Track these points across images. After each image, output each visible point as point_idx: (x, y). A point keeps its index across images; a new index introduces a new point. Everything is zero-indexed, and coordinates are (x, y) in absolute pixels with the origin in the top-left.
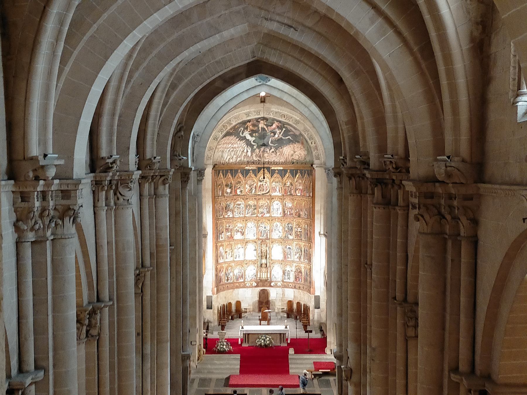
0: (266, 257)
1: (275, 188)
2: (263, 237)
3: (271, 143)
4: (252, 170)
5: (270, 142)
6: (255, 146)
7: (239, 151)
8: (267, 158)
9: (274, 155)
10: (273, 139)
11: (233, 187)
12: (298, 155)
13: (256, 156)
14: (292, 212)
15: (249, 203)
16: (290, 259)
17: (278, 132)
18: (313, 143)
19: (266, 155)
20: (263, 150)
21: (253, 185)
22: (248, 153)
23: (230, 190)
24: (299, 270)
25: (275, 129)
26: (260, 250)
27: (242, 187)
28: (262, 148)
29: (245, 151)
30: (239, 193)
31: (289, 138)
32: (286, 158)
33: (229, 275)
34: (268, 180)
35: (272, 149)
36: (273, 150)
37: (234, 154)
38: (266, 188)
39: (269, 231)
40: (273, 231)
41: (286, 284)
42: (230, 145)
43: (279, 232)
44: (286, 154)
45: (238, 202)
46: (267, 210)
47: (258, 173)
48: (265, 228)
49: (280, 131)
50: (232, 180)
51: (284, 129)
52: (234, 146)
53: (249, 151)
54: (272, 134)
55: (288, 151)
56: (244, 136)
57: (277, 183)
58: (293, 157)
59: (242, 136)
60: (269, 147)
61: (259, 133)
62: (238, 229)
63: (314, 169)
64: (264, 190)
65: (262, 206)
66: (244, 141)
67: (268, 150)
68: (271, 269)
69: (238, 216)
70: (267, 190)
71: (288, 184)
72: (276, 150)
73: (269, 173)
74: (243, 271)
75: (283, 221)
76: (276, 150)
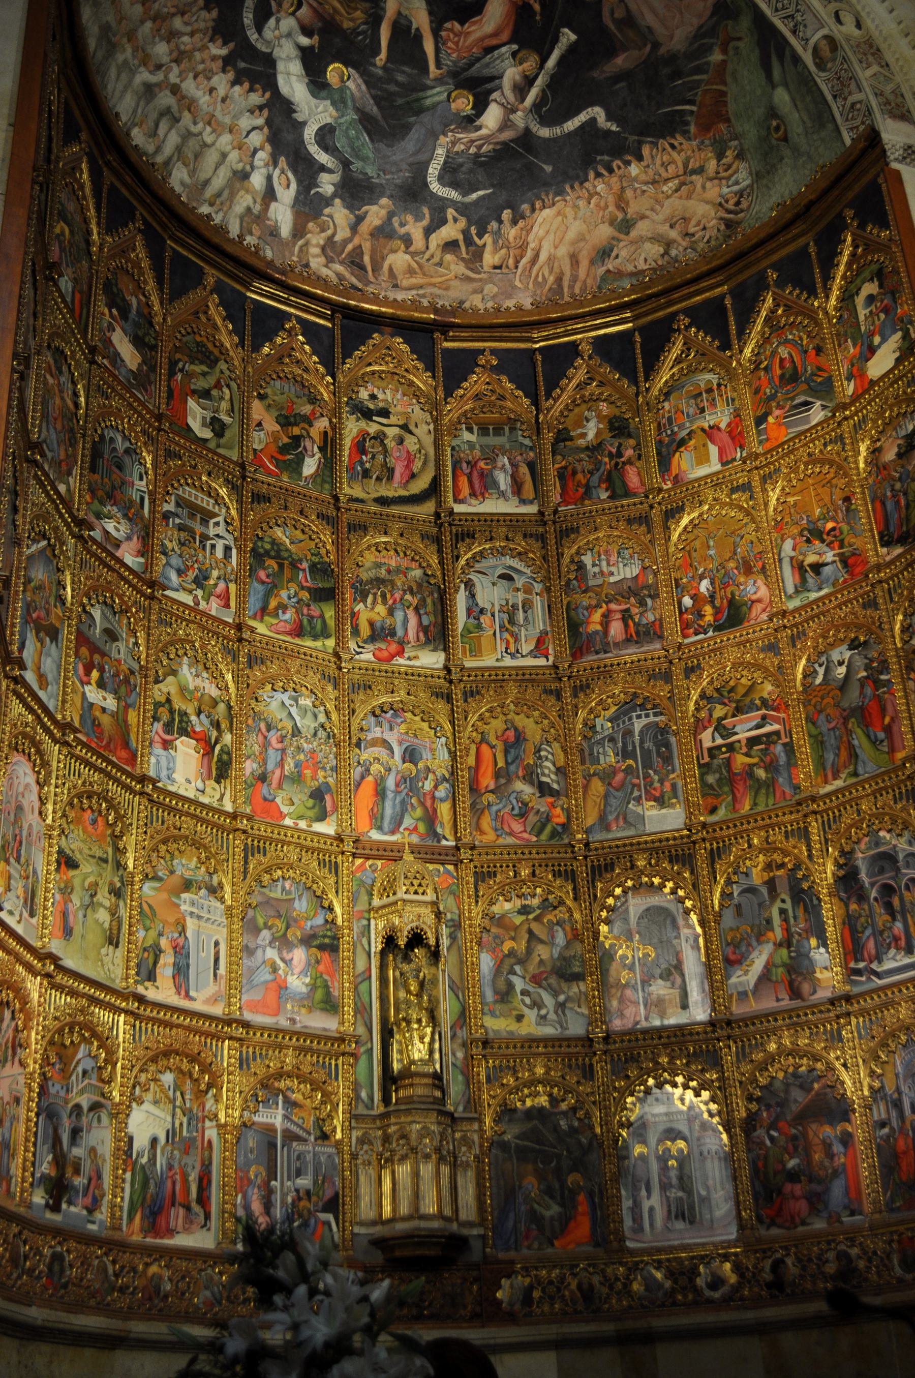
0: (433, 1019)
1: (482, 464)
2: (393, 832)
3: (441, 179)
4: (300, 320)
5: (433, 170)
6: (324, 178)
7: (211, 157)
8: (405, 283)
9: (455, 266)
10: (459, 147)
11: (163, 359)
12: (655, 239)
13: (330, 248)
14: (651, 617)
15: (279, 532)
16: (674, 1019)
17: (511, 74)
18: (848, 19)
19: (399, 260)
20: (377, 222)
21: (309, 421)
22: (273, 205)
23: (139, 359)
24: (799, 1097)
25: (490, 50)
26: (377, 946)
27: (224, 405)
28: (374, 208)
29: (257, 180)
30: (195, 424)
31: (593, 120)
32: (551, 279)
33: (76, 1133)
34: (418, 414)
35: (444, 222)
36: (449, 231)
37: (179, 149)
38: (410, 459)
39: (441, 792)
40: (487, 781)
41: (659, 1275)
42: (161, 50)
43: (544, 789)
44: (551, 259)
45: (189, 493)
46: (425, 621)
47: (344, 359)
48: (411, 755)
49: (529, 65)
50: (155, 299)
51: (568, 36)
52: (190, 86)
53: (287, 194)
54: (463, 104)
55: (571, 235)
56: (264, 49)
57: (498, 431)
58: (611, 265)
59: (253, 36)
60: (426, 211)
61: (370, 81)
62: (178, 704)
63: (887, 164)
64: (391, 472)
65: (379, 582)
66: (256, 98)
67: (415, 230)
68: (481, 1131)
69: (188, 599)
70: (413, 476)
71: (591, 430)
72: (473, 230)
73: (430, 367)
74: (211, 1133)
75: (567, 694)
76: (473, 230)
